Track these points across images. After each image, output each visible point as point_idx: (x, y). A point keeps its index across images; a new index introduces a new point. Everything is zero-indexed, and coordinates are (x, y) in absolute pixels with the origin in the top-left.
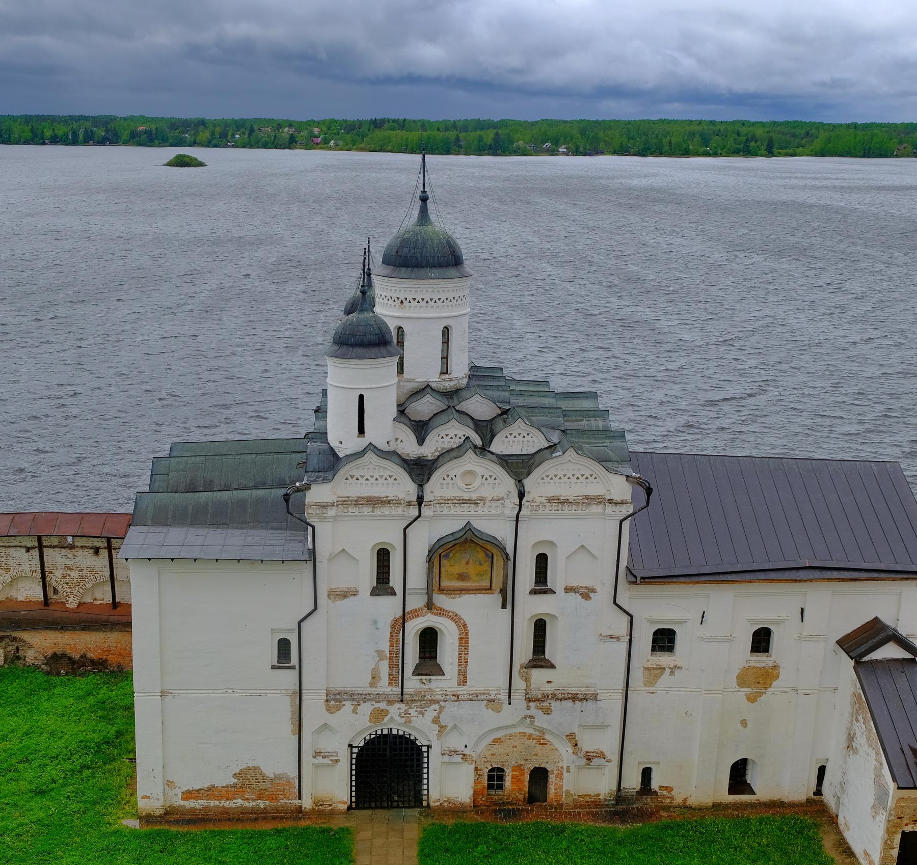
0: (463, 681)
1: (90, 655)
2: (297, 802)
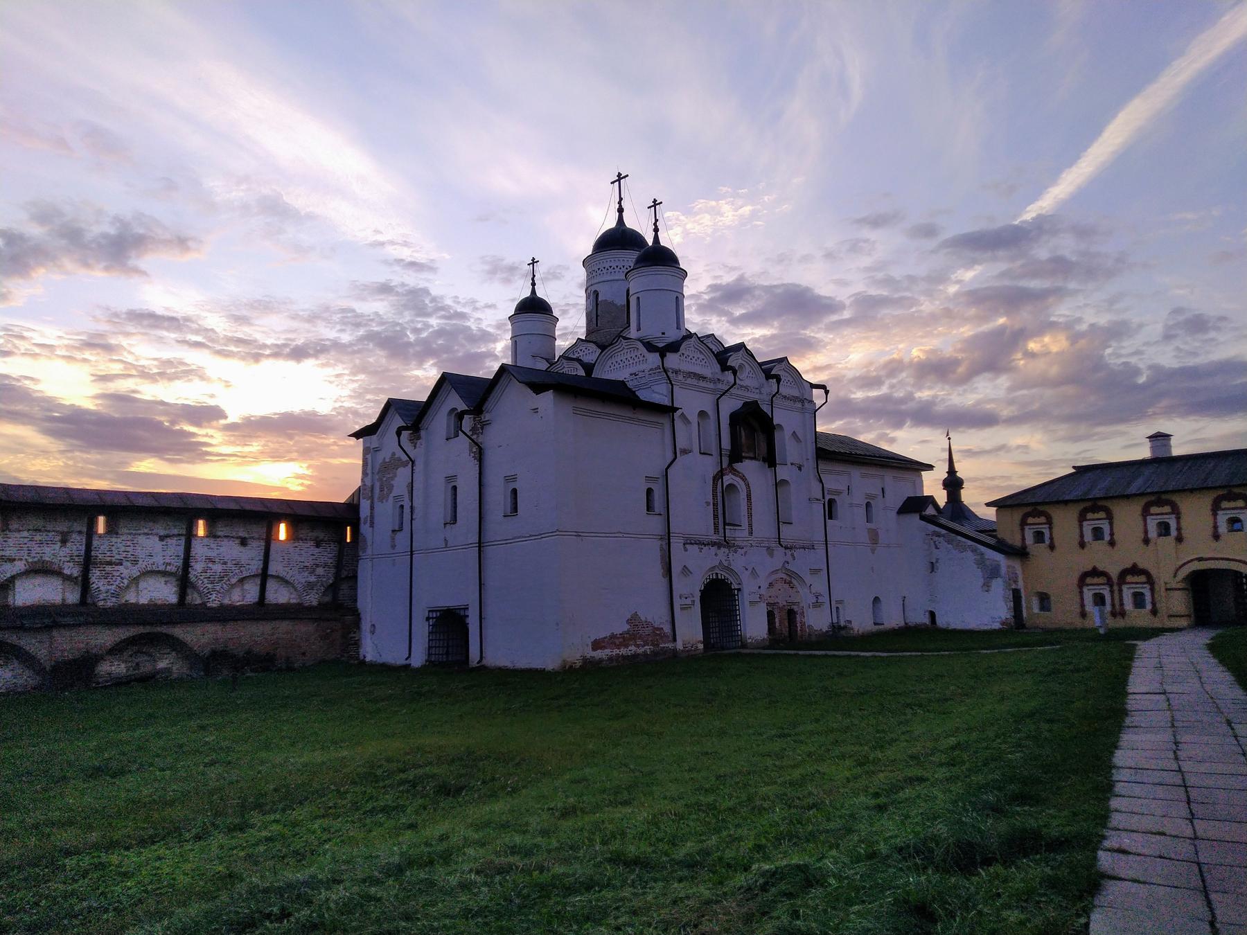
0: (751, 533)
1: (256, 650)
2: (670, 645)
